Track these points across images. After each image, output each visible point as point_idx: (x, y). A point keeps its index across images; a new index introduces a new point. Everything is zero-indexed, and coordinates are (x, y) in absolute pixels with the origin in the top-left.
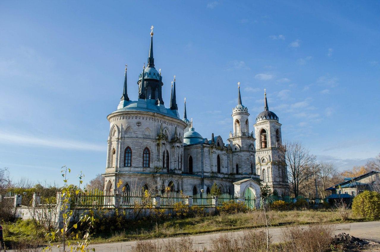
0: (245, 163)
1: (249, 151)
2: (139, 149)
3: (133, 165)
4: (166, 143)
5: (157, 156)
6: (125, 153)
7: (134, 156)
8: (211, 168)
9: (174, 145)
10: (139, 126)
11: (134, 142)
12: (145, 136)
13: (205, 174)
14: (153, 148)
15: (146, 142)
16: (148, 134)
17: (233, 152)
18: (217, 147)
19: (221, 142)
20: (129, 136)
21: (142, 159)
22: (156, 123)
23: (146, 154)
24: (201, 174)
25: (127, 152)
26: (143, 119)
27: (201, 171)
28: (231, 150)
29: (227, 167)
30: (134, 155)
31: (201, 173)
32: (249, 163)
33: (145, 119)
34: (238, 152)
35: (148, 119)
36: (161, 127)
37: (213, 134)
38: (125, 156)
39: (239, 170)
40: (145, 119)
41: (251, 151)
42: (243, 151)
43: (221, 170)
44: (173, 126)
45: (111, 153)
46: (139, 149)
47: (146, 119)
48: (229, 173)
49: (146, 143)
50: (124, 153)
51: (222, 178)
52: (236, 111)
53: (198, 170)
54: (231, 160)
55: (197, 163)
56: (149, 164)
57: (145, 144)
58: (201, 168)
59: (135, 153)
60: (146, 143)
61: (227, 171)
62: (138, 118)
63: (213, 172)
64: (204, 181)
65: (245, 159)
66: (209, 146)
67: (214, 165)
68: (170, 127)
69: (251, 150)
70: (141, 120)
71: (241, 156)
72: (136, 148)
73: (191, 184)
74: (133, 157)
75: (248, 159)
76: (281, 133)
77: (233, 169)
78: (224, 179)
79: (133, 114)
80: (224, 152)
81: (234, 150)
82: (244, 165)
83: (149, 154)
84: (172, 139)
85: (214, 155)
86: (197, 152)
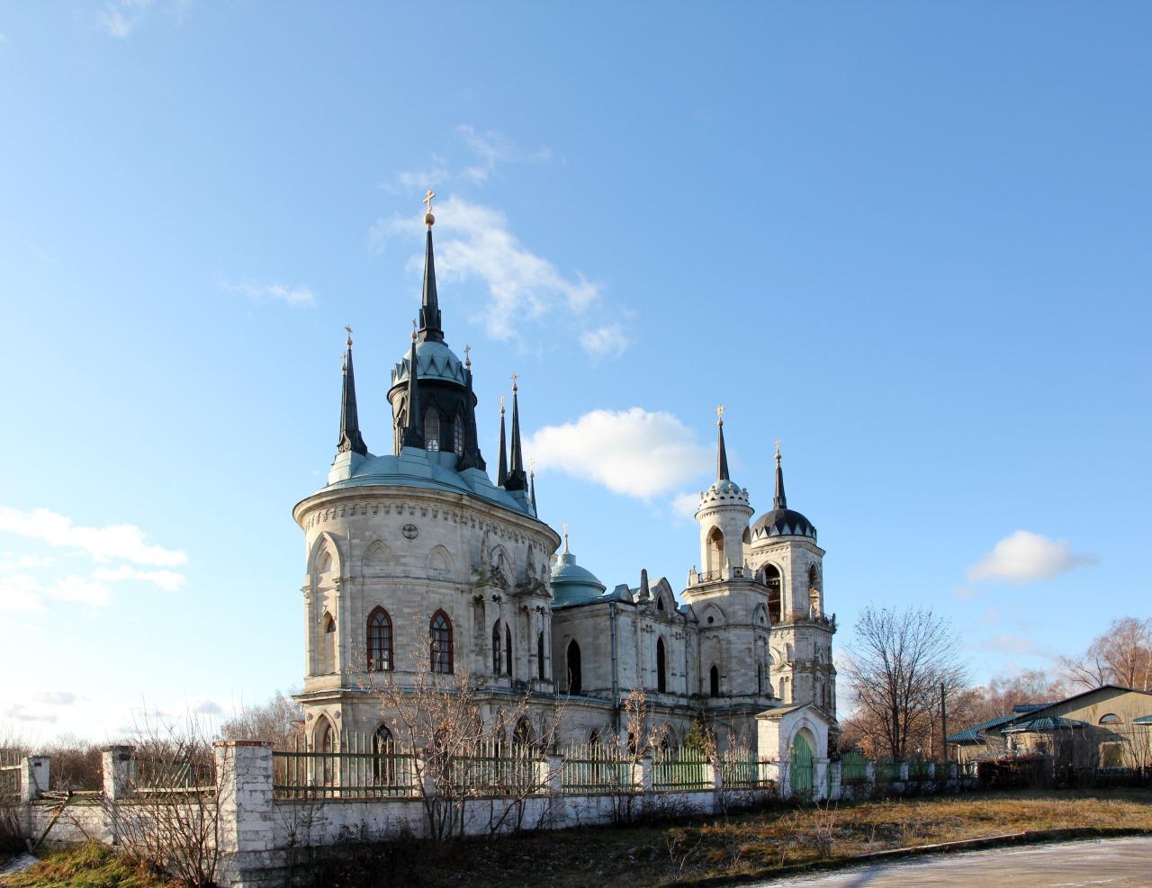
0: (741, 662)
1: (754, 627)
4: (502, 595)
5: (476, 638)
6: (370, 627)
7: (399, 638)
9: (525, 604)
11: (399, 593)
12: (432, 573)
14: (462, 616)
15: (438, 593)
16: (443, 567)
17: (702, 630)
18: (657, 612)
19: (669, 597)
20: (378, 572)
22: (467, 531)
23: (440, 629)
24: (611, 696)
25: (375, 623)
26: (424, 515)
27: (610, 686)
28: (696, 622)
29: (686, 675)
30: (401, 635)
31: (610, 693)
32: (753, 663)
33: (430, 514)
34: (719, 628)
35: (440, 516)
36: (483, 542)
37: (644, 572)
38: (370, 639)
39: (719, 683)
41: (759, 627)
42: (736, 626)
43: (669, 684)
44: (520, 544)
45: (322, 630)
47: (435, 516)
48: (690, 693)
50: (365, 627)
51: (672, 709)
52: (713, 499)
53: (599, 684)
55: (595, 662)
56: (451, 664)
58: (610, 677)
59: (400, 627)
60: (438, 596)
62: (406, 513)
63: (647, 691)
68: (510, 546)
69: (759, 623)
70: (417, 520)
71: (729, 642)
72: (405, 610)
73: (583, 726)
74: (399, 640)
75: (750, 649)
76: (821, 577)
77: (701, 681)
78: (677, 711)
79: (387, 496)
80: (676, 629)
81: (704, 623)
82: (738, 668)
83: (450, 630)
84: (518, 586)
85: (648, 635)
86: (595, 628)
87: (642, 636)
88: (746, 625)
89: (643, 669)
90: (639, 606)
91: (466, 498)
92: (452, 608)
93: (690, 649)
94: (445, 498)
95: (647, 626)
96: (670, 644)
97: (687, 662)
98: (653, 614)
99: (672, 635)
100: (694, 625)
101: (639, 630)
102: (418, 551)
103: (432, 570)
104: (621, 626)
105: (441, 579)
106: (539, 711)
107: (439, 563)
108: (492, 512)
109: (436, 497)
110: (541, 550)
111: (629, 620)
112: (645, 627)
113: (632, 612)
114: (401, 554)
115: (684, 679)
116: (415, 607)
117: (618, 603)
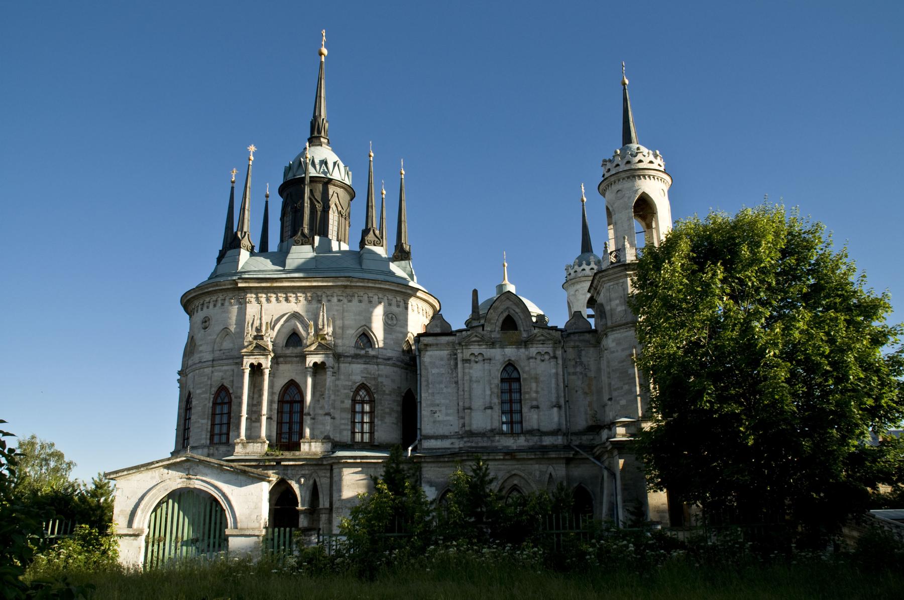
2: (204, 393)
3: (192, 442)
10: (205, 328)
12: (217, 354)
13: (427, 444)
15: (220, 371)
16: (231, 346)
21: (206, 423)
26: (215, 306)
37: (475, 293)
40: (219, 304)
46: (204, 393)
47: (223, 304)
48: (581, 423)
49: (221, 374)
54: (592, 374)
57: (217, 376)
61: (556, 419)
62: (205, 308)
63: (471, 434)
64: (424, 469)
65: (623, 362)
66: (451, 338)
67: (478, 403)
72: (198, 391)
80: (533, 350)
83: (230, 403)
85: (475, 366)
87: (464, 368)
88: (627, 324)
89: (464, 409)
90: (458, 334)
91: (240, 281)
92: (233, 381)
93: (578, 369)
94: (224, 287)
95: (472, 354)
96: (527, 369)
97: (566, 386)
98: (482, 341)
99: (529, 358)
100: (588, 336)
101: (460, 365)
102: (210, 337)
103: (218, 352)
104: (426, 364)
105: (224, 357)
106: (307, 472)
108: (275, 285)
109: (217, 288)
110: (360, 301)
111: (445, 353)
113: (448, 343)
114: (200, 343)
115: (555, 410)
117: (422, 339)
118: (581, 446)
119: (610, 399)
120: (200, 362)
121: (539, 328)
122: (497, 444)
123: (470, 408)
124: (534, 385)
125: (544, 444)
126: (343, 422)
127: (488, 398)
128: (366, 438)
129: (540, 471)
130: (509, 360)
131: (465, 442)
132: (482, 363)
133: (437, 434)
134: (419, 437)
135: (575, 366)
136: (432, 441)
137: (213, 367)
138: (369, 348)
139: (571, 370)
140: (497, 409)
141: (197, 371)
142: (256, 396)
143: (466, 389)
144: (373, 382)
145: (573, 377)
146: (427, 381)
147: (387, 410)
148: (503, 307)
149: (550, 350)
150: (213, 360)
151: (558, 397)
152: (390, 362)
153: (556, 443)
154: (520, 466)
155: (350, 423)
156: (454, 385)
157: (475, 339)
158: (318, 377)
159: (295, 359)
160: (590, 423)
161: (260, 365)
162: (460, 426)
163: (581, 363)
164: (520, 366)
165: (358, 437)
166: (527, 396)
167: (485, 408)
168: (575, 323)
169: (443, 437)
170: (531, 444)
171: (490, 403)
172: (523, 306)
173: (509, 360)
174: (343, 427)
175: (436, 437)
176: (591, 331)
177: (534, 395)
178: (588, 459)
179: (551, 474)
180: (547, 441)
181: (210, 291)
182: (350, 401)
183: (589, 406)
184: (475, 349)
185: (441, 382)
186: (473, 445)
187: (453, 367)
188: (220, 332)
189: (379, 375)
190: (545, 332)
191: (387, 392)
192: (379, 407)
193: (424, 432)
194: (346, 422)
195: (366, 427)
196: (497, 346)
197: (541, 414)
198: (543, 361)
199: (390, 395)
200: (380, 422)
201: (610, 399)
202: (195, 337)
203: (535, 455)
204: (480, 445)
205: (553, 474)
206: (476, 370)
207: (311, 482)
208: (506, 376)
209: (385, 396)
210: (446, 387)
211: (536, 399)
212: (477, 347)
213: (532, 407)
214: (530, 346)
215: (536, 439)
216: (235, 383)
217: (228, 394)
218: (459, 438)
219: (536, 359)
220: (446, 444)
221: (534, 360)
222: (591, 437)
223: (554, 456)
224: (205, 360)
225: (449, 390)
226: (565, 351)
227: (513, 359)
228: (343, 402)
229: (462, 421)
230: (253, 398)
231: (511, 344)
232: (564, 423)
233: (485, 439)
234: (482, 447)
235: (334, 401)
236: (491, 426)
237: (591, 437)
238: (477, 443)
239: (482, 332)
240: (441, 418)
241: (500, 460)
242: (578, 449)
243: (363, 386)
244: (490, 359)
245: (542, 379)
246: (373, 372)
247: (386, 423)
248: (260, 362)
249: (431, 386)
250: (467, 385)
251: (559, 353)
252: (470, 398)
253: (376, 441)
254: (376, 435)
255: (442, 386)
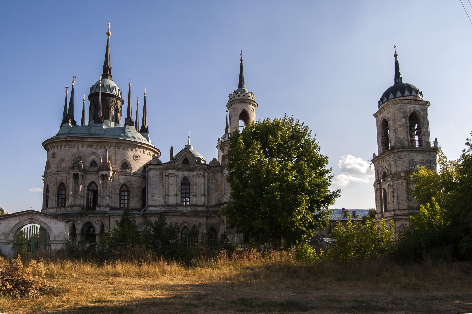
8: (165, 199)
10: (53, 157)
12: (59, 169)
13: (150, 209)
14: (71, 183)
16: (65, 166)
48: (214, 202)
49: (61, 177)
57: (59, 178)
60: (61, 177)
61: (203, 201)
63: (168, 205)
66: (161, 166)
67: (171, 193)
80: (195, 173)
87: (166, 179)
89: (166, 195)
90: (164, 165)
92: (66, 181)
95: (170, 173)
96: (192, 180)
97: (208, 188)
98: (174, 168)
99: (193, 176)
100: (218, 168)
101: (164, 177)
102: (55, 162)
104: (150, 176)
105: (62, 170)
107: (64, 165)
111: (158, 173)
112: (168, 174)
113: (159, 169)
115: (203, 197)
116: (53, 183)
117: (148, 166)
118: (213, 212)
119: (225, 194)
120: (52, 172)
121: (198, 164)
122: (178, 210)
123: (168, 195)
124: (195, 187)
125: (198, 210)
126: (116, 199)
127: (175, 191)
128: (126, 206)
129: (196, 221)
130: (185, 176)
131: (166, 209)
132: (174, 177)
133: (154, 205)
134: (146, 206)
135: (212, 180)
136: (152, 208)
137: (57, 174)
138: (127, 169)
139: (211, 181)
140: (179, 196)
141: (51, 176)
142: (77, 187)
143: (166, 187)
144: (129, 183)
145: (211, 184)
146: (150, 183)
147: (135, 195)
148: (183, 155)
149: (202, 173)
150: (57, 172)
151: (204, 192)
152: (137, 175)
153: (202, 210)
154: (187, 218)
155: (118, 200)
156: (162, 186)
157: (171, 167)
158: (105, 180)
159: (94, 172)
160: (217, 202)
161: (78, 174)
162: (164, 202)
163: (215, 179)
164: (190, 179)
165: (122, 206)
166: (192, 191)
167: (174, 195)
168: (213, 162)
169: (156, 206)
170: (193, 210)
171: (177, 193)
172: (192, 154)
173: (185, 176)
174: (115, 201)
175: (153, 206)
176: (220, 166)
177: (195, 191)
178: (215, 216)
179: (200, 222)
180: (199, 209)
181: (55, 141)
182: (119, 191)
183: (217, 196)
184: (171, 172)
185: (156, 184)
186: (169, 210)
187: (161, 178)
188: (60, 159)
189: (131, 180)
190: (200, 166)
191: (135, 187)
192: (132, 194)
193: (149, 204)
194: (117, 199)
195: (126, 202)
196: (180, 170)
197: (197, 198)
198: (199, 177)
199: (136, 189)
200: (132, 200)
201: (225, 194)
202: (49, 161)
203: (194, 214)
204: (172, 210)
205: (201, 222)
206: (172, 180)
207: (101, 223)
208: (184, 182)
209: (134, 189)
210: (158, 186)
211: (196, 192)
212: (172, 170)
213: (194, 196)
214: (194, 171)
215: (195, 208)
216: (67, 182)
217: (65, 186)
218: (163, 207)
219: (196, 176)
220: (158, 209)
221: (195, 177)
222: (217, 208)
223: (201, 215)
224: (54, 171)
225: (160, 187)
226: (209, 174)
227: (187, 176)
228: (115, 191)
229: (164, 200)
230: (76, 188)
231: (186, 170)
232: (207, 202)
233: (174, 208)
234: (172, 211)
235: (112, 190)
236: (177, 202)
237: (217, 208)
238: (170, 209)
239: (174, 165)
240: (156, 199)
241: (179, 216)
242: (211, 213)
243: (124, 185)
244: (177, 176)
245: (198, 184)
246: (129, 179)
247: (134, 200)
248: (78, 173)
249: (152, 186)
250: (167, 186)
251: (206, 174)
252: (168, 191)
253: (130, 207)
254: (130, 205)
255: (157, 186)
